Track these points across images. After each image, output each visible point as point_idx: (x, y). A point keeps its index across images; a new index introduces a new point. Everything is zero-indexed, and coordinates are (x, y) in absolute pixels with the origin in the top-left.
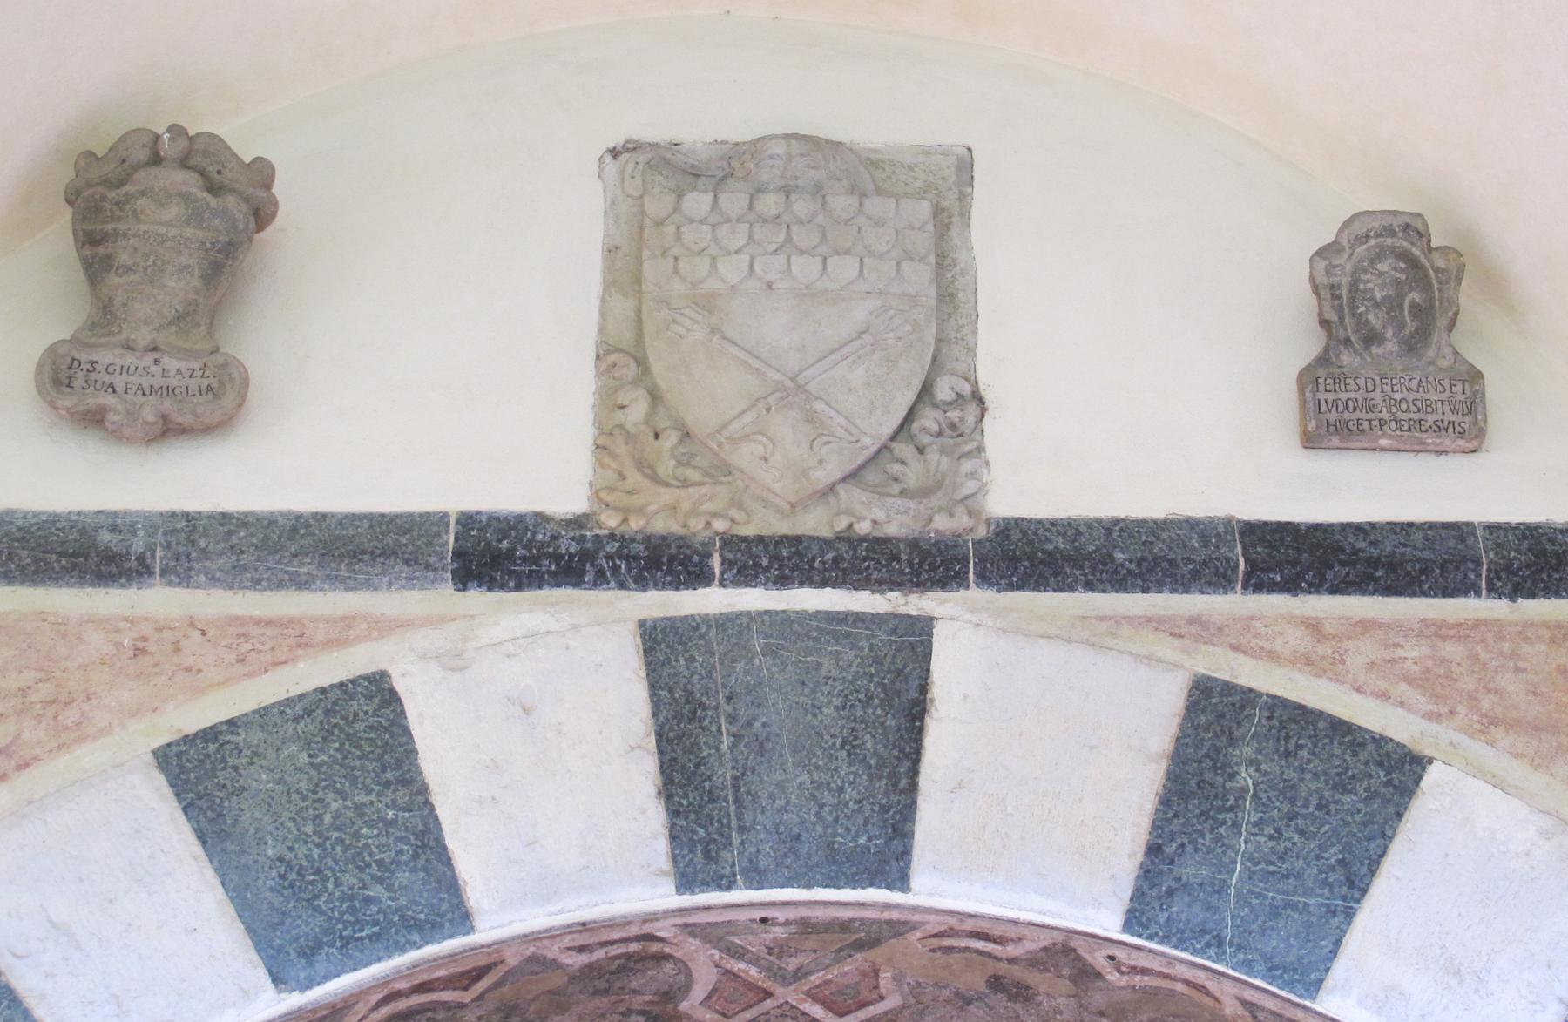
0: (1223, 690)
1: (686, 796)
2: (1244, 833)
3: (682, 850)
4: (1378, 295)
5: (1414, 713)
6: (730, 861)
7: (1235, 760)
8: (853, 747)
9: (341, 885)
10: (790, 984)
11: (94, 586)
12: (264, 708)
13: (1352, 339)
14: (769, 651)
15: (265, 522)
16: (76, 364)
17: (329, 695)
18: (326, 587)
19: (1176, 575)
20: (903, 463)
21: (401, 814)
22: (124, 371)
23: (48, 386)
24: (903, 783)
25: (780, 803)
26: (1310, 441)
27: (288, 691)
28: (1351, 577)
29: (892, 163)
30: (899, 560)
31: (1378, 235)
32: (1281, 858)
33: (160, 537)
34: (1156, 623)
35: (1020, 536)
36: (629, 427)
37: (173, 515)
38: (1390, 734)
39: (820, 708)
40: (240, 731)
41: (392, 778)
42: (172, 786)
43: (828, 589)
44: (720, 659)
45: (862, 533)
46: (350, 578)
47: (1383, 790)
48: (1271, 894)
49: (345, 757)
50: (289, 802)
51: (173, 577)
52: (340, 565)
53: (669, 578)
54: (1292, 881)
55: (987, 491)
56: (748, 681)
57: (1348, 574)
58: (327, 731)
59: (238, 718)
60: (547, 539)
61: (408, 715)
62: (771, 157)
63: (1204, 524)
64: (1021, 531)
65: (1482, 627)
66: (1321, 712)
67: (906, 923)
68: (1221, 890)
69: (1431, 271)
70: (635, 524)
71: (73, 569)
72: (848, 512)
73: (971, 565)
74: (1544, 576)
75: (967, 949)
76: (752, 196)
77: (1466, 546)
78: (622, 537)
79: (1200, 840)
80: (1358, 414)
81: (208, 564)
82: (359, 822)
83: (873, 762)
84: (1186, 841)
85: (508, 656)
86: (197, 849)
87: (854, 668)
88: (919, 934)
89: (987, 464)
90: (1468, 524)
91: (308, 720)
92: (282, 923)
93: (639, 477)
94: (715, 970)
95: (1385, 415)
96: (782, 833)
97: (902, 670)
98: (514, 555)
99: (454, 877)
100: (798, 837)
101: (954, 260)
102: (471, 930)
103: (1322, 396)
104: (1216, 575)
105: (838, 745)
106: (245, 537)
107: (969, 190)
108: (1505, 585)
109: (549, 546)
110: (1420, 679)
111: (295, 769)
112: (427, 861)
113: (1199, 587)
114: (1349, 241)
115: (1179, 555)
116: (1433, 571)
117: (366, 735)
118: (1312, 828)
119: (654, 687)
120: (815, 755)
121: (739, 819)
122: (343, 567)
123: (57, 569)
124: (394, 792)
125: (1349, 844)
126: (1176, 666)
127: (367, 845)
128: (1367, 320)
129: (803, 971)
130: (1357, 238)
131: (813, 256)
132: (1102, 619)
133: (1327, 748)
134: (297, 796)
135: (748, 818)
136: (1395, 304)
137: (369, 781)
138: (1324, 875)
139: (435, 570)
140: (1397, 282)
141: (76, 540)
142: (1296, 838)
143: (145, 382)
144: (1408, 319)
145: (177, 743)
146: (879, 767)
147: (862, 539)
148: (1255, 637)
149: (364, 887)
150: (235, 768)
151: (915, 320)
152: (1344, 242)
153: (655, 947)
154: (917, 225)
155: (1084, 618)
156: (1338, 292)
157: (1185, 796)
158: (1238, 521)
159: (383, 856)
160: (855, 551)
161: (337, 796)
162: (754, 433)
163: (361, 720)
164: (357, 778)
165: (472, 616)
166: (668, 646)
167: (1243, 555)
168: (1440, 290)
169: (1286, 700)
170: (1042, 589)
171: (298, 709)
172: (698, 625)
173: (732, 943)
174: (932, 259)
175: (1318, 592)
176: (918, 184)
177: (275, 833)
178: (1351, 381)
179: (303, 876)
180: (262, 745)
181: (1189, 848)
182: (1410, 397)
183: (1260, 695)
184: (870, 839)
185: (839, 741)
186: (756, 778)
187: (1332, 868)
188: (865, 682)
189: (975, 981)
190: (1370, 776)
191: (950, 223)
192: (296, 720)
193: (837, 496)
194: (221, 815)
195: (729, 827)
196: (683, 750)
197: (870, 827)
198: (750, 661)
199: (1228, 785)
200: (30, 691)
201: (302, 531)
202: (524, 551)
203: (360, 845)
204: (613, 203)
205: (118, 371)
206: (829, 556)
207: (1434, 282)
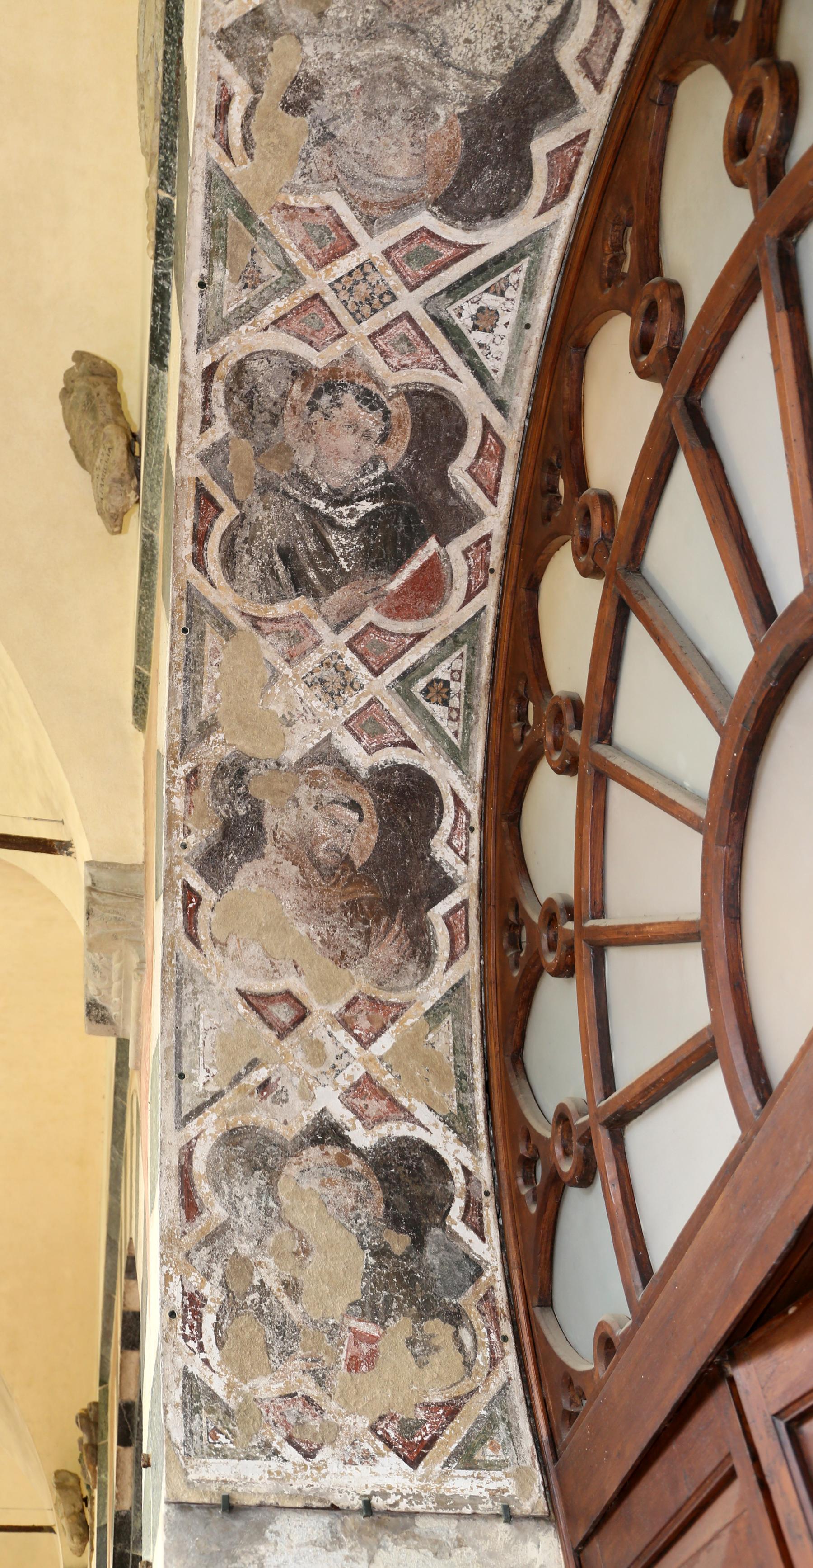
10: (301, 278)
67: (210, 174)
75: (245, 125)
88: (226, 165)
153: (223, 370)
173: (234, 312)
189: (293, 124)
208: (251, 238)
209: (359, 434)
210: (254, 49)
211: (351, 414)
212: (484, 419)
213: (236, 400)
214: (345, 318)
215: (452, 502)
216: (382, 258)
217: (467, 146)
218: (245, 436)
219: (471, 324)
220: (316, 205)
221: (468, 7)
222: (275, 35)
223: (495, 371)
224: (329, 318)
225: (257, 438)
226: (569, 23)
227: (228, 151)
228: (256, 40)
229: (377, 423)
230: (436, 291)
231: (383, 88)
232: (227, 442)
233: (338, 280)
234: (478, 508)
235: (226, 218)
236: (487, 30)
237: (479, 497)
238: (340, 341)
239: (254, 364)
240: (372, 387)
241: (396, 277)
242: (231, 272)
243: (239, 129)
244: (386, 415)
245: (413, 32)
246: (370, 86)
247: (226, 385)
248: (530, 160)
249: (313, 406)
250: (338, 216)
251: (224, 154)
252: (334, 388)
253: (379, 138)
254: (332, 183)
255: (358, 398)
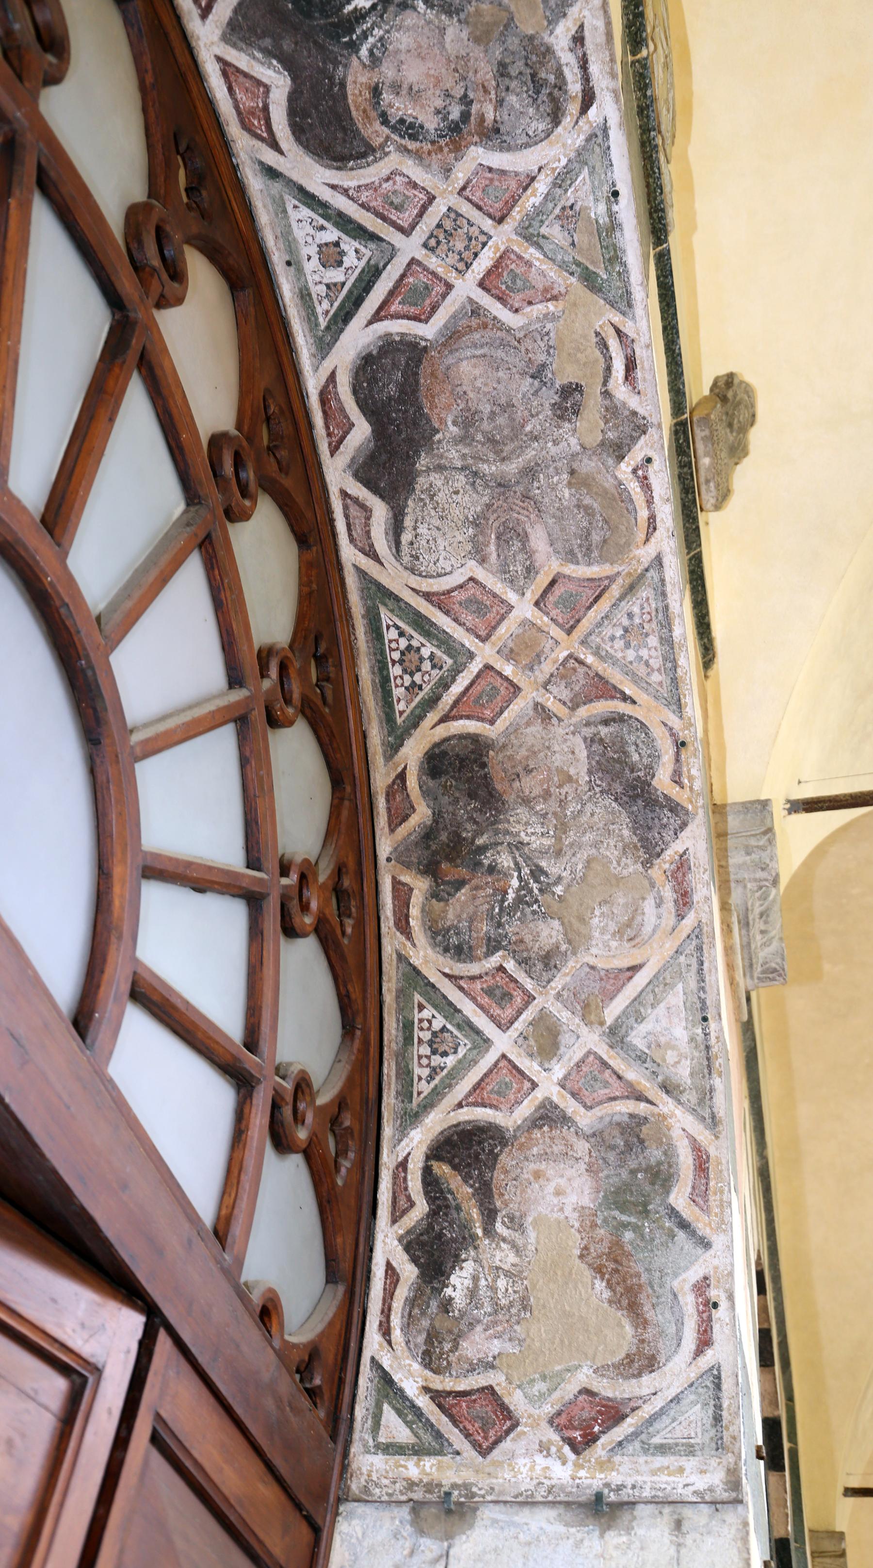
10: (520, 235)
129: (541, 241)
189: (568, 374)
208: (579, 258)
209: (405, 86)
210: (616, 426)
211: (422, 106)
212: (281, 153)
213: (552, 78)
214: (465, 208)
215: (267, 42)
216: (452, 281)
217: (420, 408)
218: (531, 38)
219: (342, 245)
220: (528, 309)
221: (467, 518)
222: (602, 444)
223: (295, 207)
224: (481, 203)
225: (517, 41)
226: (391, 533)
227: (618, 332)
228: (616, 434)
229: (391, 106)
230: (389, 267)
231: (506, 432)
232: (550, 23)
233: (484, 244)
234: (234, 46)
235: (606, 269)
236: (446, 506)
237: (240, 60)
238: (461, 183)
239: (542, 126)
240: (412, 145)
241: (432, 267)
242: (590, 217)
243: (613, 355)
244: (384, 119)
245: (500, 485)
246: (517, 429)
247: (566, 92)
248: (365, 415)
249: (466, 101)
250: (505, 306)
251: (622, 328)
252: (450, 129)
253: (495, 389)
254: (520, 335)
255: (422, 127)
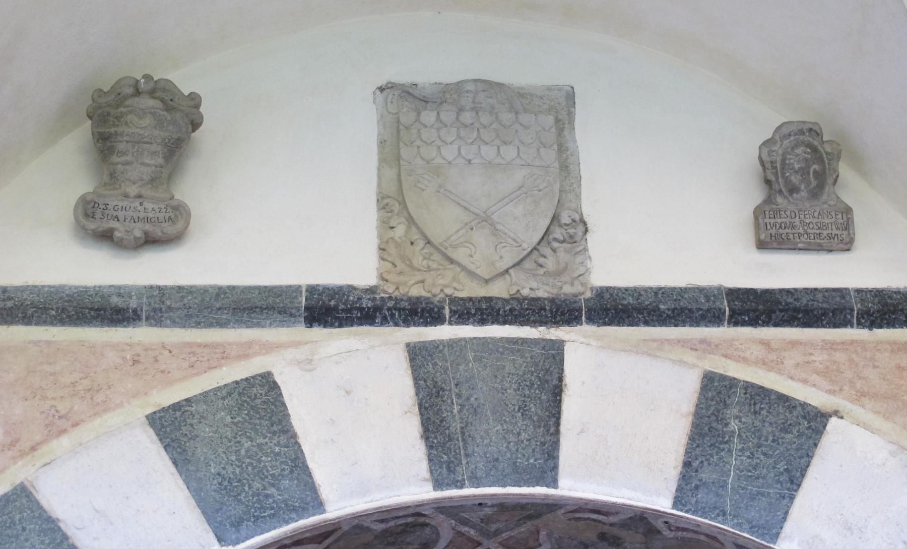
0: (719, 379)
1: (436, 438)
2: (734, 455)
3: (435, 467)
4: (797, 166)
5: (821, 390)
6: (461, 472)
7: (728, 416)
8: (524, 411)
9: (252, 487)
11: (109, 326)
12: (205, 392)
13: (783, 190)
14: (478, 359)
15: (202, 291)
16: (97, 205)
17: (240, 385)
18: (236, 326)
19: (693, 317)
20: (545, 257)
21: (283, 449)
22: (124, 209)
23: (81, 218)
24: (552, 430)
25: (486, 441)
26: (762, 245)
27: (218, 383)
28: (785, 318)
29: (531, 95)
30: (545, 310)
31: (795, 134)
32: (755, 468)
33: (145, 300)
34: (682, 343)
35: (609, 297)
36: (396, 238)
37: (151, 287)
38: (809, 402)
39: (506, 390)
40: (193, 405)
41: (276, 430)
42: (158, 435)
43: (507, 326)
44: (451, 364)
45: (525, 295)
46: (249, 321)
47: (806, 432)
48: (750, 488)
49: (251, 419)
50: (222, 443)
51: (152, 321)
52: (243, 314)
53: (421, 320)
54: (761, 480)
55: (591, 272)
56: (467, 376)
57: (783, 316)
58: (240, 404)
59: (192, 398)
60: (355, 300)
61: (284, 395)
62: (467, 92)
63: (707, 290)
64: (610, 294)
65: (855, 344)
66: (772, 390)
68: (724, 486)
69: (824, 154)
70: (403, 290)
71: (98, 317)
72: (516, 284)
73: (584, 312)
74: (887, 316)
75: (588, 519)
76: (457, 113)
77: (846, 301)
78: (396, 298)
79: (712, 459)
80: (787, 230)
81: (171, 314)
82: (260, 454)
83: (535, 419)
84: (704, 459)
85: (337, 363)
86: (173, 469)
87: (523, 368)
88: (562, 511)
89: (590, 257)
90: (846, 289)
91: (230, 398)
92: (221, 509)
93: (403, 266)
94: (452, 532)
95: (801, 231)
96: (488, 457)
97: (549, 369)
98: (338, 308)
99: (313, 482)
100: (497, 460)
101: (567, 147)
102: (324, 511)
103: (767, 220)
104: (714, 317)
105: (516, 410)
106: (191, 299)
107: (573, 109)
108: (866, 321)
109: (356, 303)
110: (824, 372)
111: (224, 425)
112: (298, 474)
113: (705, 323)
114: (780, 138)
115: (694, 306)
116: (828, 314)
117: (262, 407)
118: (770, 452)
119: (416, 380)
120: (504, 415)
121: (465, 450)
122: (245, 315)
123: (89, 317)
124: (278, 437)
125: (790, 460)
126: (694, 366)
127: (265, 466)
128: (791, 181)
130: (784, 136)
131: (492, 146)
132: (654, 341)
133: (776, 409)
134: (226, 440)
135: (470, 449)
136: (805, 172)
137: (264, 431)
138: (778, 477)
139: (295, 316)
140: (806, 160)
141: (99, 302)
142: (762, 457)
143: (135, 215)
144: (812, 180)
145: (159, 411)
146: (538, 421)
147: (525, 299)
148: (735, 350)
149: (265, 489)
150: (192, 425)
151: (548, 180)
152: (777, 138)
153: (421, 520)
154: (547, 128)
155: (644, 340)
156: (775, 165)
157: (702, 435)
158: (725, 288)
159: (274, 472)
160: (521, 305)
161: (248, 440)
162: (466, 242)
163: (259, 399)
164: (258, 430)
165: (316, 342)
166: (422, 357)
167: (728, 306)
168: (829, 164)
169: (753, 384)
170: (621, 325)
171: (224, 393)
172: (438, 345)
174: (555, 147)
175: (768, 325)
176: (545, 107)
177: (215, 460)
178: (783, 213)
179: (231, 483)
180: (205, 412)
181: (705, 463)
182: (815, 221)
183: (739, 381)
184: (535, 460)
185: (517, 408)
186: (473, 428)
187: (782, 473)
188: (529, 376)
190: (800, 424)
191: (564, 127)
192: (223, 398)
193: (510, 275)
194: (184, 451)
195: (460, 455)
196: (433, 413)
197: (535, 453)
198: (467, 365)
199: (725, 429)
200: (77, 384)
201: (222, 296)
202: (343, 306)
203: (261, 466)
204: (382, 116)
205: (120, 209)
206: (508, 308)
207: (826, 160)
213: (400, 528)
